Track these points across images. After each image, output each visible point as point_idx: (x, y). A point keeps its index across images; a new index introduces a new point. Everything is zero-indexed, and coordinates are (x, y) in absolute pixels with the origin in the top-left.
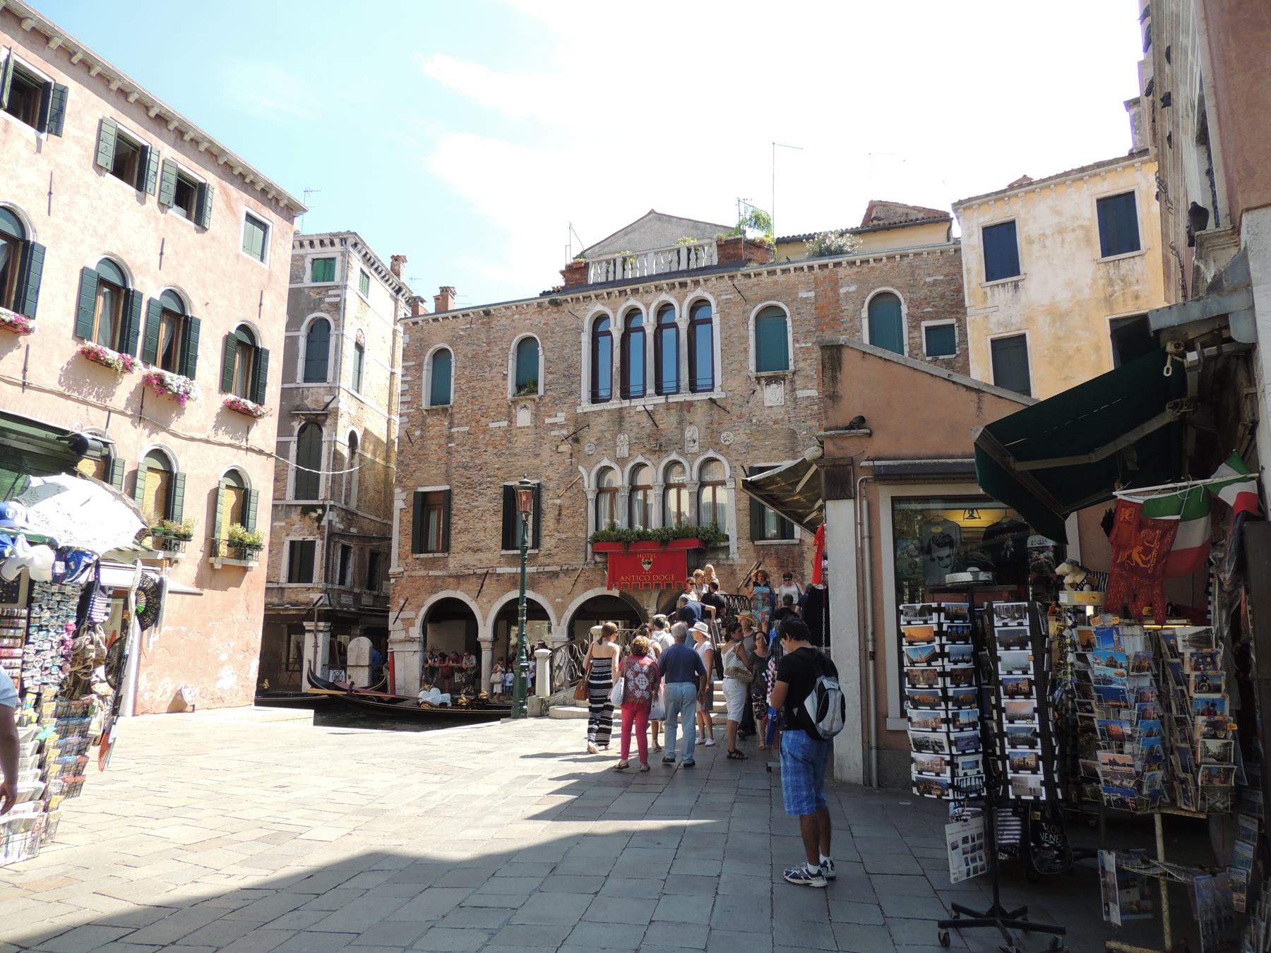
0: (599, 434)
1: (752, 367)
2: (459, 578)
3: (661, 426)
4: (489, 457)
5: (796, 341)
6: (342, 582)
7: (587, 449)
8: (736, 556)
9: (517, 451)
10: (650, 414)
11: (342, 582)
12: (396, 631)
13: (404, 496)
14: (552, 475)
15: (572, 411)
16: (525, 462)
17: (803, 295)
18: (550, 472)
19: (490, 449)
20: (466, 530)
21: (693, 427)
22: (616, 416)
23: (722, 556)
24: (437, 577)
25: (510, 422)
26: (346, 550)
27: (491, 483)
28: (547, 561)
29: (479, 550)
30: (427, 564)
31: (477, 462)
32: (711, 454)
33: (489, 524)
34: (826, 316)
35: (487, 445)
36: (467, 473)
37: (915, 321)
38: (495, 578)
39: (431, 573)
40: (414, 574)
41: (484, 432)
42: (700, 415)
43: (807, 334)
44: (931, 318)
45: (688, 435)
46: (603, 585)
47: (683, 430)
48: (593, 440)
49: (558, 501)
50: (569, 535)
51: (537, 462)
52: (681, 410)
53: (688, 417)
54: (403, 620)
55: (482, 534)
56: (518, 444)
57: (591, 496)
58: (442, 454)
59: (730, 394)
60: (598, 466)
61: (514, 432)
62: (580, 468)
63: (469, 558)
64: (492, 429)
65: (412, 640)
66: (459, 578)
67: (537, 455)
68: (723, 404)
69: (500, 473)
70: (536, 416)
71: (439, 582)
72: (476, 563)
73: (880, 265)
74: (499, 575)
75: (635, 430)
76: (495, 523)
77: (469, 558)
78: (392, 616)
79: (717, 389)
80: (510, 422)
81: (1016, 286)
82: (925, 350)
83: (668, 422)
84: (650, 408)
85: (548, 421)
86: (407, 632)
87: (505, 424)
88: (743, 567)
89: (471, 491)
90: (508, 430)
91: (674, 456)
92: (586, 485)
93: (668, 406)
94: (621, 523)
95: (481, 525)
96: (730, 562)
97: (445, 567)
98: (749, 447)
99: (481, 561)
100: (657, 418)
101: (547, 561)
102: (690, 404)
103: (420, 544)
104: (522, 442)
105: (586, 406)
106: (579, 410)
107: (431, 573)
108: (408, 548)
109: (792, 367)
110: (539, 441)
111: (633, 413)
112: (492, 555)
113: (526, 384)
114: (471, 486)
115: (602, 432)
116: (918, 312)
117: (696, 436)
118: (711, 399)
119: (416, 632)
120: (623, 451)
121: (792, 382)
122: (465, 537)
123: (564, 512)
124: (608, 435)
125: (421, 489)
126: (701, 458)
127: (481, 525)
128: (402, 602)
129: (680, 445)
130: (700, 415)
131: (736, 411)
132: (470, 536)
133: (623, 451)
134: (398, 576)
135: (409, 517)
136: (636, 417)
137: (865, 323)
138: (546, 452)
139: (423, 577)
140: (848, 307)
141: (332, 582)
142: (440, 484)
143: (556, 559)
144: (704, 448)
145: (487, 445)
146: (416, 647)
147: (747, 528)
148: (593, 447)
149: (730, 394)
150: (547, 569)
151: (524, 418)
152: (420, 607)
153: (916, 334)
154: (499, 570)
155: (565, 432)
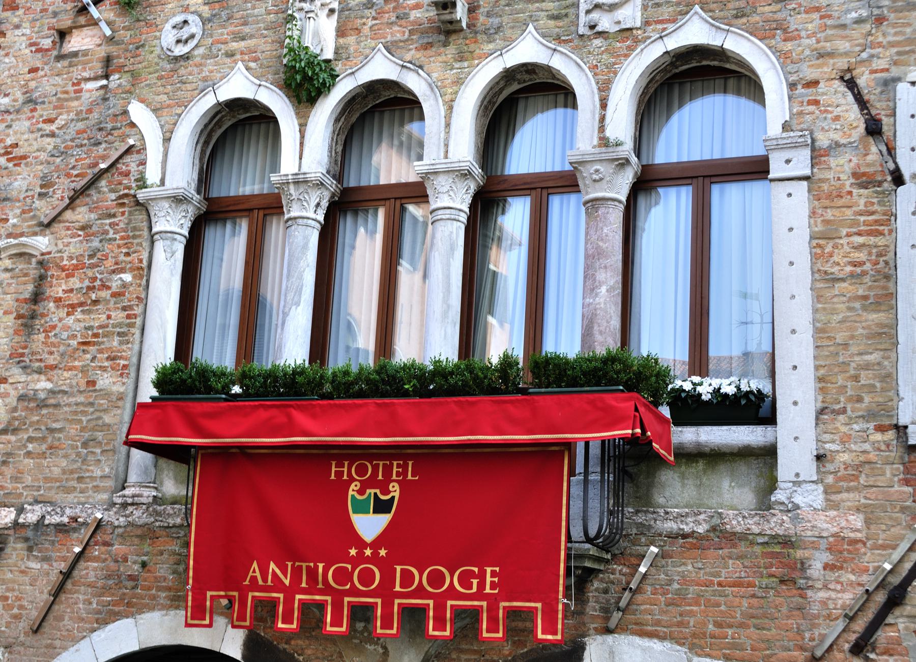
7: (168, 37)
8: (810, 498)
49: (42, 243)
50: (66, 378)
57: (174, 223)
60: (207, 102)
62: (138, 112)
92: (152, 174)
94: (291, 348)
123: (58, 289)
148: (195, 27)
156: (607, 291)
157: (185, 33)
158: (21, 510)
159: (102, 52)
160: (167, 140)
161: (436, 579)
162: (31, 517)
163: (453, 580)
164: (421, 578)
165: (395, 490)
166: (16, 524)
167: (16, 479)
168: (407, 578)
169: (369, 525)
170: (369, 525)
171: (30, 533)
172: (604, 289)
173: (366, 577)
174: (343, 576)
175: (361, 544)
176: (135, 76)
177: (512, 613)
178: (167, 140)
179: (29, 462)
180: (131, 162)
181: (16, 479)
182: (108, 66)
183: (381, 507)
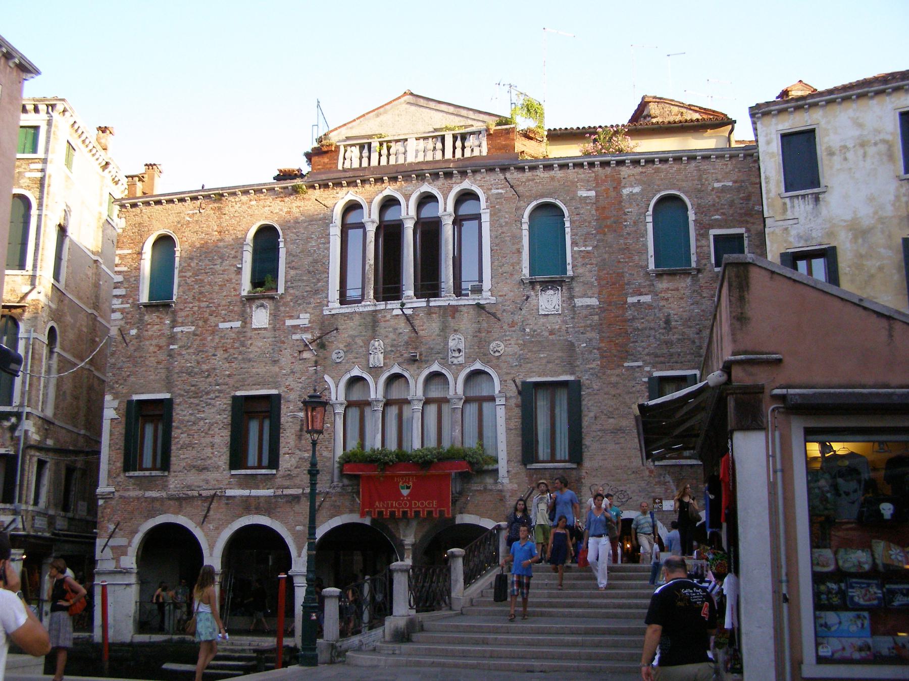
0: (349, 340)
1: (526, 271)
2: (181, 501)
3: (421, 333)
4: (218, 361)
5: (574, 243)
6: (36, 503)
7: (334, 356)
9: (252, 356)
10: (408, 318)
11: (36, 503)
12: (104, 560)
13: (116, 404)
14: (293, 385)
15: (317, 312)
16: (260, 369)
17: (583, 193)
18: (290, 381)
19: (220, 353)
20: (191, 445)
21: (457, 337)
22: (369, 319)
23: (489, 480)
24: (154, 499)
25: (245, 322)
26: (41, 464)
27: (220, 391)
28: (287, 483)
30: (144, 484)
31: (204, 367)
32: (478, 366)
33: (217, 440)
34: (608, 218)
35: (216, 348)
36: (193, 380)
37: (703, 229)
38: (224, 501)
39: (149, 494)
40: (127, 494)
41: (213, 333)
42: (466, 322)
43: (587, 237)
44: (720, 227)
45: (452, 344)
46: (352, 511)
47: (446, 339)
48: (341, 346)
51: (277, 369)
52: (444, 315)
53: (452, 323)
54: (113, 548)
56: (253, 348)
58: (162, 356)
59: (500, 299)
61: (249, 334)
62: (327, 378)
63: (193, 478)
64: (222, 330)
65: (126, 572)
66: (181, 501)
67: (275, 362)
68: (493, 311)
69: (231, 382)
70: (274, 316)
71: (157, 505)
72: (201, 484)
73: (665, 166)
74: (229, 498)
75: (391, 335)
76: (222, 437)
77: (193, 478)
78: (100, 543)
79: (486, 294)
80: (245, 322)
81: (817, 199)
82: (713, 261)
83: (430, 328)
84: (408, 312)
85: (289, 322)
86: (118, 561)
87: (238, 324)
88: (513, 492)
89: (196, 401)
90: (241, 332)
91: (436, 367)
93: (429, 311)
95: (208, 440)
96: (499, 487)
97: (165, 487)
98: (522, 360)
99: (207, 482)
100: (417, 323)
101: (287, 483)
102: (455, 310)
103: (131, 460)
104: (257, 346)
105: (334, 306)
106: (326, 312)
107: (149, 494)
108: (119, 464)
109: (570, 273)
110: (278, 344)
111: (388, 317)
112: (219, 476)
113: (264, 275)
114: (196, 395)
115: (353, 337)
116: (706, 220)
117: (462, 346)
118: (478, 305)
119: (130, 561)
120: (377, 359)
121: (570, 289)
124: (359, 341)
125: (136, 397)
126: (468, 370)
127: (208, 440)
128: (112, 527)
129: (443, 355)
130: (466, 322)
131: (507, 318)
132: (194, 452)
133: (377, 359)
134: (107, 497)
135: (121, 429)
136: (392, 322)
137: (650, 227)
138: (286, 358)
139: (138, 499)
140: (632, 210)
141: (27, 503)
142: (159, 392)
144: (470, 359)
145: (216, 348)
146: (133, 579)
147: (518, 449)
148: (342, 354)
149: (500, 299)
150: (287, 492)
151: (261, 318)
152: (135, 532)
153: (704, 242)
154: (230, 493)
155: (307, 337)
157: (340, 355)
159: (314, 358)
160: (337, 387)
161: (422, 504)
163: (426, 503)
164: (419, 504)
165: (411, 484)
166: (303, 493)
167: (301, 481)
168: (415, 504)
169: (405, 492)
170: (405, 492)
173: (406, 504)
174: (400, 504)
175: (403, 496)
176: (325, 367)
177: (440, 511)
178: (337, 387)
180: (326, 393)
182: (316, 362)
183: (408, 488)
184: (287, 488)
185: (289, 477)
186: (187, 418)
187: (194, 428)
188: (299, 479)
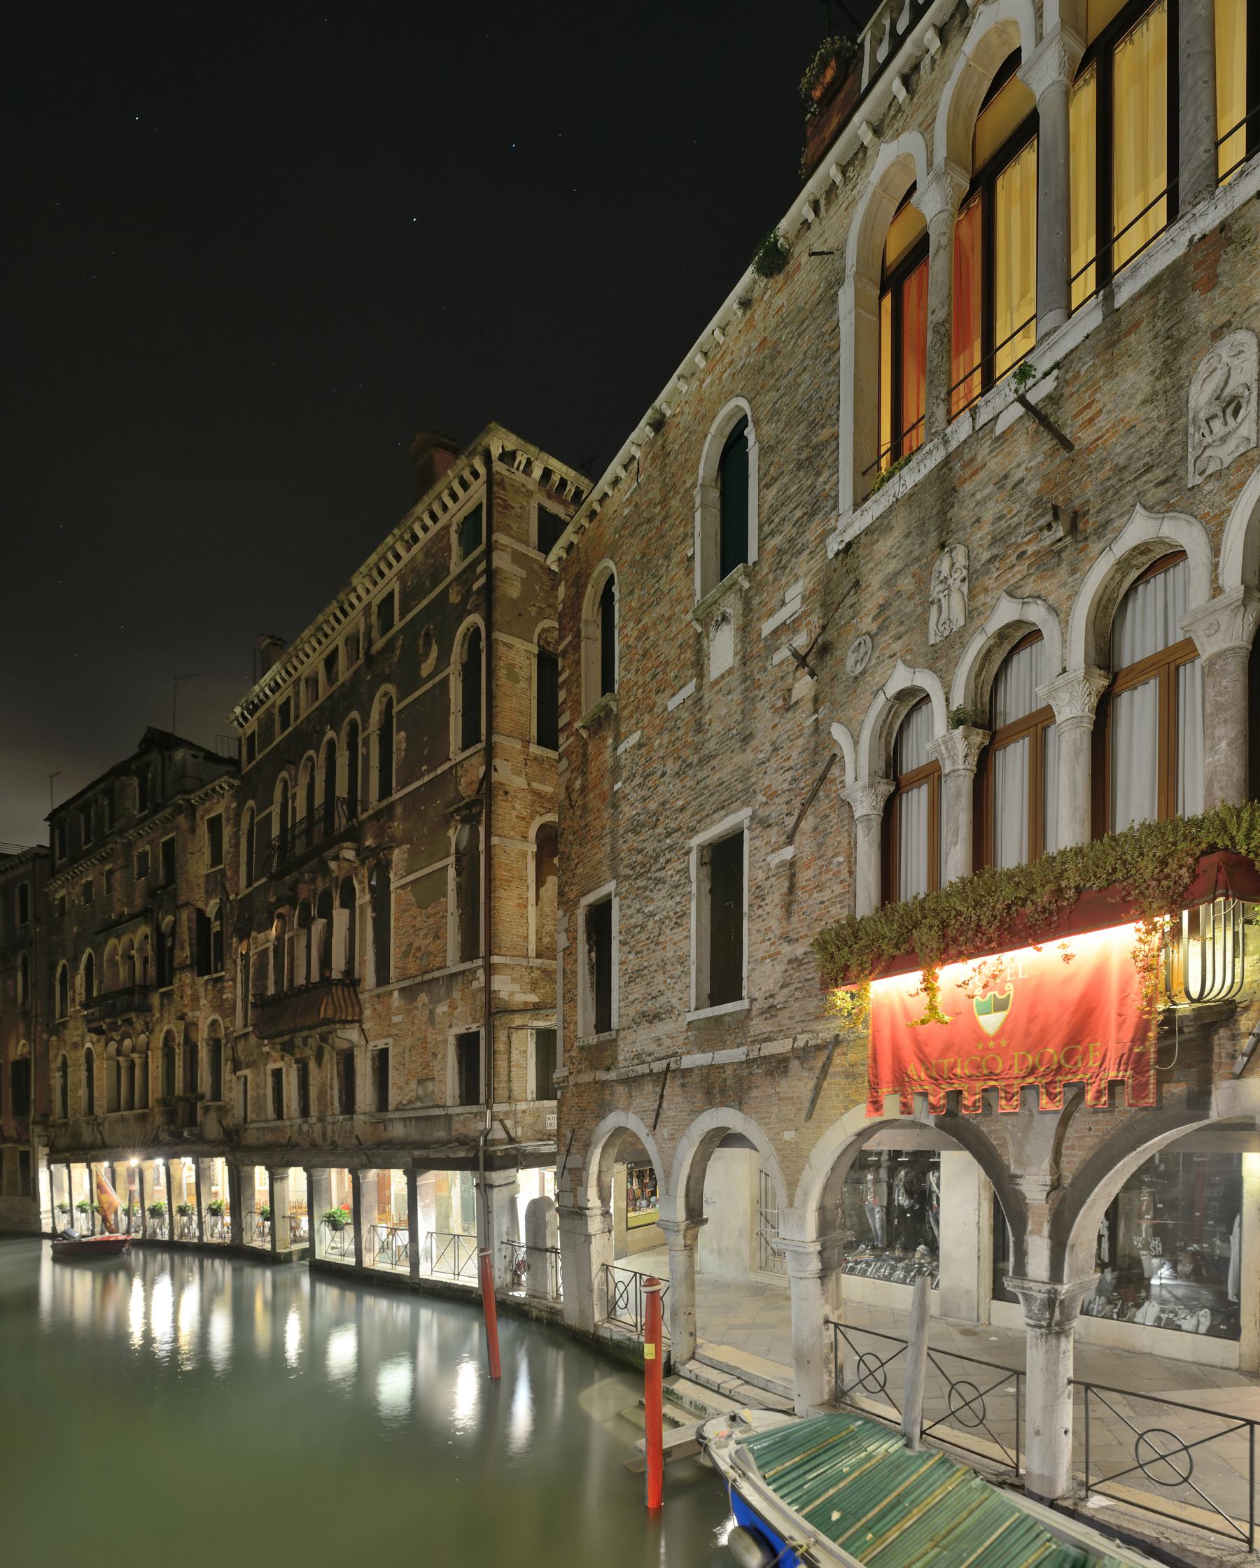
29: (657, 1017)
55: (660, 977)
69: (684, 818)
122: (638, 991)
143: (783, 1017)
156: (1228, 744)
158: (795, 1040)
162: (800, 1044)
171: (801, 1054)
172: (1224, 744)
179: (797, 1005)
181: (791, 1018)
184: (768, 1039)
185: (770, 1011)
186: (633, 921)
187: (643, 936)
188: (786, 1013)
